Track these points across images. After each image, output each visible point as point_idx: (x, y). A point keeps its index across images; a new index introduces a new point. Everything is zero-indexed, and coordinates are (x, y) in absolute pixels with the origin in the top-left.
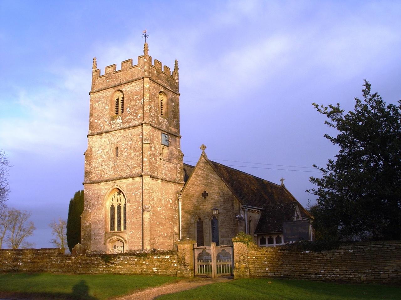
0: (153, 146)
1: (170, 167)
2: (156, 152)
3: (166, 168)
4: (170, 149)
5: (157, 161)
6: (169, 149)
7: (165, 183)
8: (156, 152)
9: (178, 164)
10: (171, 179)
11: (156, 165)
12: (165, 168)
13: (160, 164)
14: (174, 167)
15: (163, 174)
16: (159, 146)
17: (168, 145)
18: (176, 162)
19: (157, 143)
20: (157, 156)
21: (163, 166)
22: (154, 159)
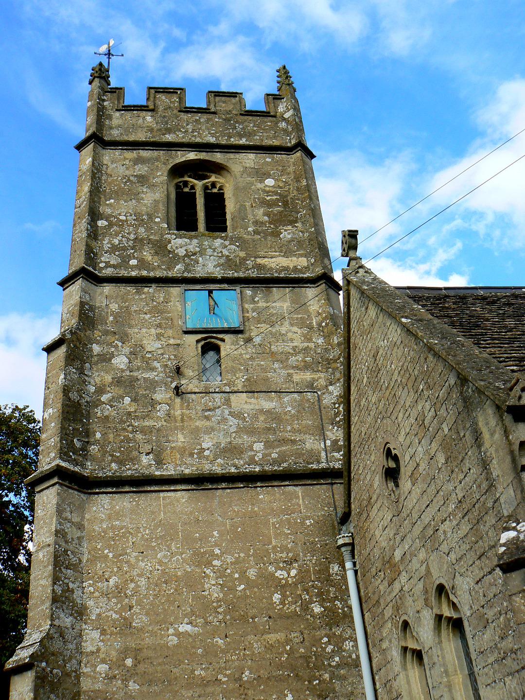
0: (127, 350)
1: (269, 412)
2: (153, 369)
3: (232, 421)
4: (257, 340)
5: (153, 403)
6: (249, 340)
7: (222, 495)
8: (153, 369)
9: (331, 388)
10: (275, 462)
11: (147, 423)
12: (224, 420)
13: (178, 413)
14: (300, 407)
15: (207, 453)
16: (172, 341)
17: (235, 324)
18: (314, 380)
19: (153, 331)
20: (152, 385)
21: (207, 418)
22: (127, 400)
